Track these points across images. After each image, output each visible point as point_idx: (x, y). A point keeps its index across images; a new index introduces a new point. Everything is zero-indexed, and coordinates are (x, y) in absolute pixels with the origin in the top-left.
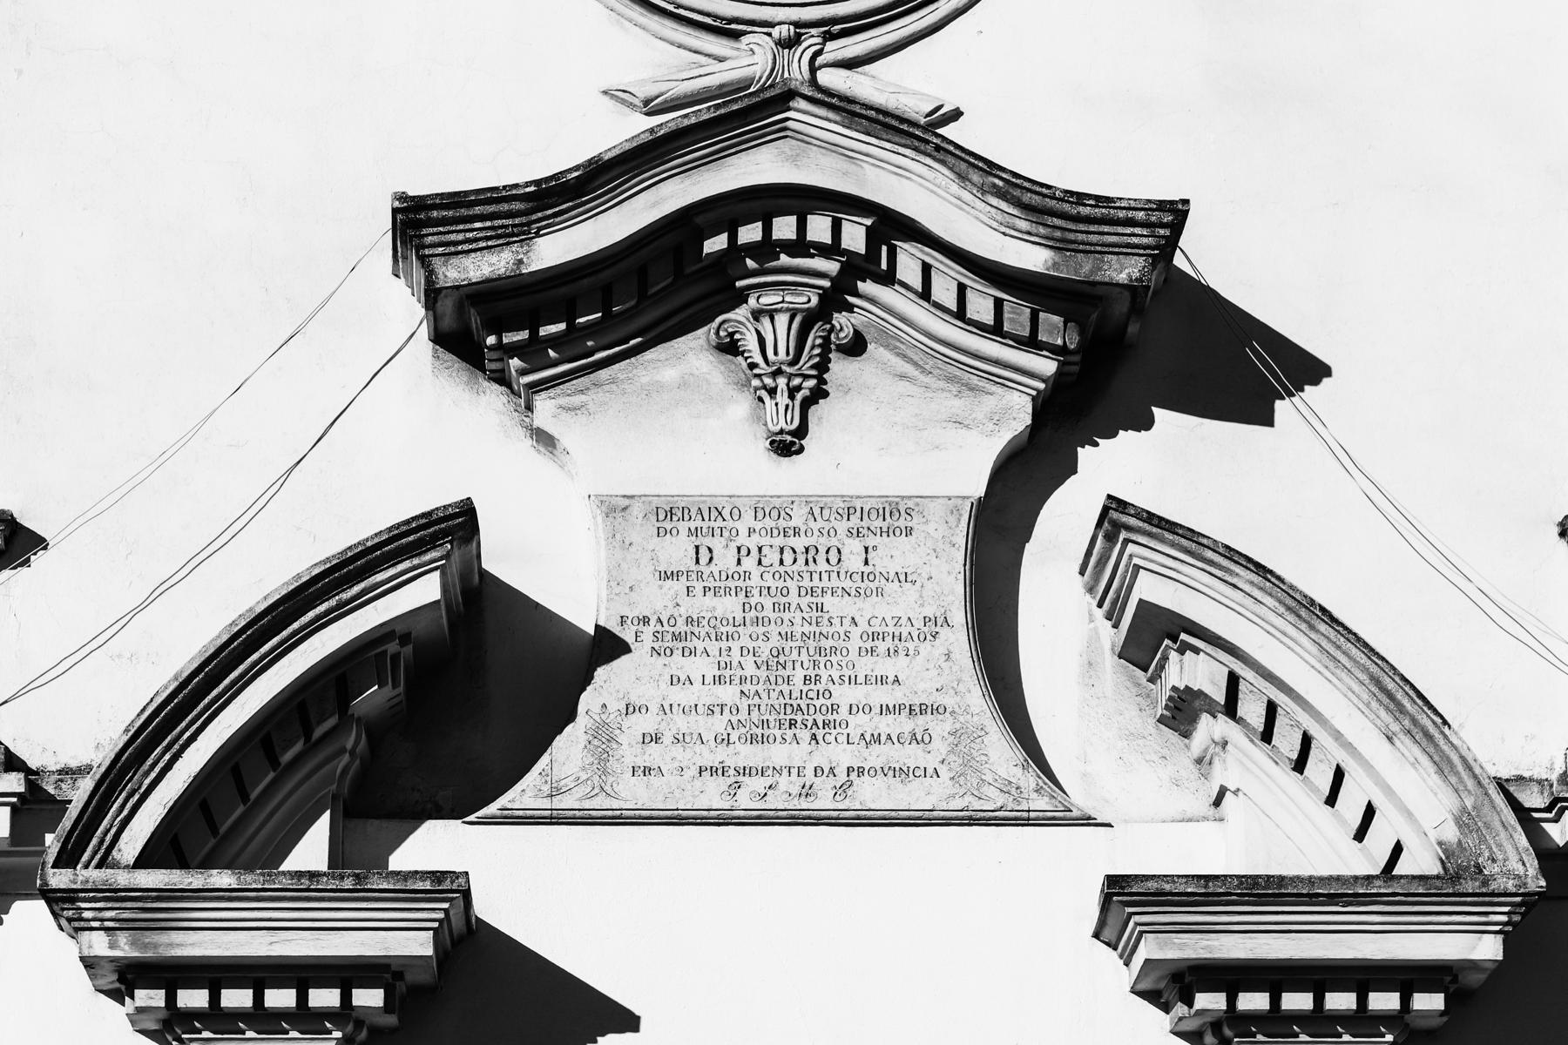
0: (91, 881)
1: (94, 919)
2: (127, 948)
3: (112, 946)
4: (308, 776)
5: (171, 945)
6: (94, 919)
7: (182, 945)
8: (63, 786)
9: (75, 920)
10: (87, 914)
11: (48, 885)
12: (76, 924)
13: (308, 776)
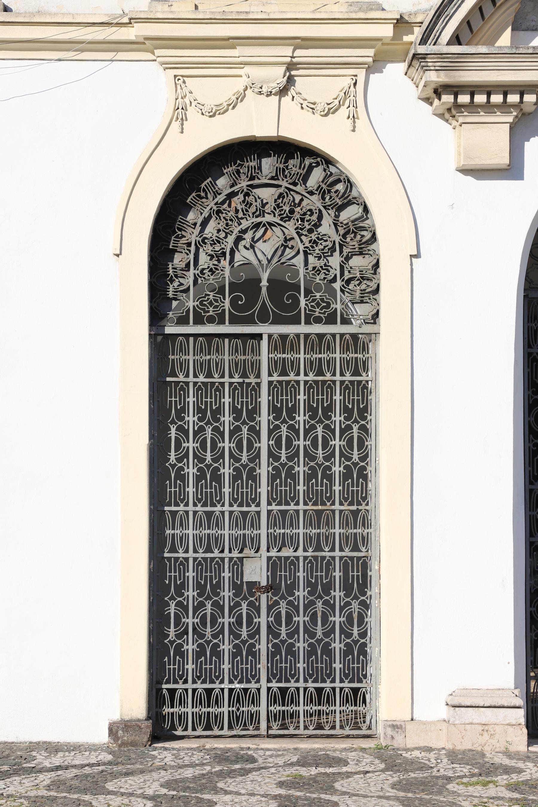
0: (433, 50)
1: (432, 66)
2: (443, 77)
3: (438, 77)
4: (504, 12)
5: (460, 76)
6: (432, 66)
7: (464, 76)
8: (411, 16)
9: (425, 66)
10: (430, 64)
11: (417, 52)
12: (425, 68)
13: (504, 12)
